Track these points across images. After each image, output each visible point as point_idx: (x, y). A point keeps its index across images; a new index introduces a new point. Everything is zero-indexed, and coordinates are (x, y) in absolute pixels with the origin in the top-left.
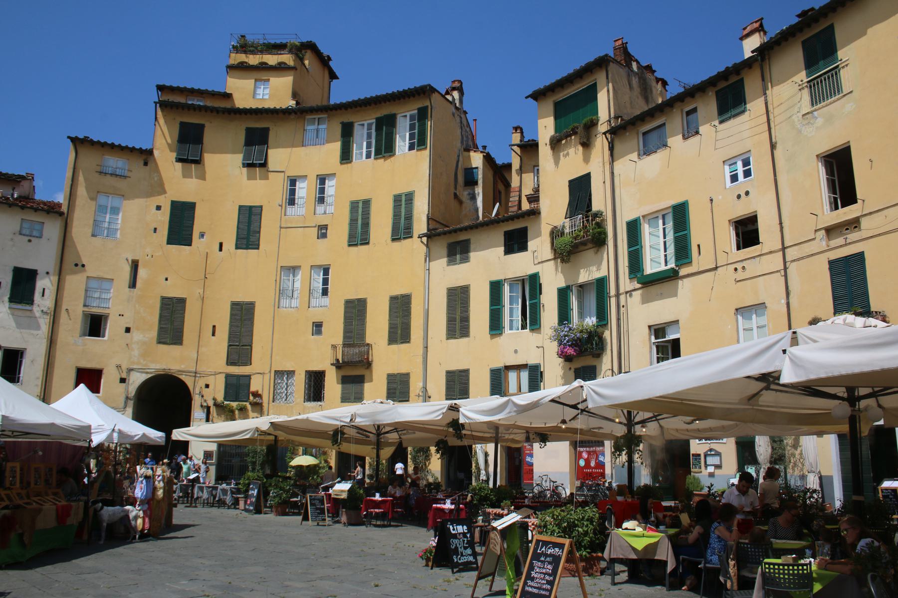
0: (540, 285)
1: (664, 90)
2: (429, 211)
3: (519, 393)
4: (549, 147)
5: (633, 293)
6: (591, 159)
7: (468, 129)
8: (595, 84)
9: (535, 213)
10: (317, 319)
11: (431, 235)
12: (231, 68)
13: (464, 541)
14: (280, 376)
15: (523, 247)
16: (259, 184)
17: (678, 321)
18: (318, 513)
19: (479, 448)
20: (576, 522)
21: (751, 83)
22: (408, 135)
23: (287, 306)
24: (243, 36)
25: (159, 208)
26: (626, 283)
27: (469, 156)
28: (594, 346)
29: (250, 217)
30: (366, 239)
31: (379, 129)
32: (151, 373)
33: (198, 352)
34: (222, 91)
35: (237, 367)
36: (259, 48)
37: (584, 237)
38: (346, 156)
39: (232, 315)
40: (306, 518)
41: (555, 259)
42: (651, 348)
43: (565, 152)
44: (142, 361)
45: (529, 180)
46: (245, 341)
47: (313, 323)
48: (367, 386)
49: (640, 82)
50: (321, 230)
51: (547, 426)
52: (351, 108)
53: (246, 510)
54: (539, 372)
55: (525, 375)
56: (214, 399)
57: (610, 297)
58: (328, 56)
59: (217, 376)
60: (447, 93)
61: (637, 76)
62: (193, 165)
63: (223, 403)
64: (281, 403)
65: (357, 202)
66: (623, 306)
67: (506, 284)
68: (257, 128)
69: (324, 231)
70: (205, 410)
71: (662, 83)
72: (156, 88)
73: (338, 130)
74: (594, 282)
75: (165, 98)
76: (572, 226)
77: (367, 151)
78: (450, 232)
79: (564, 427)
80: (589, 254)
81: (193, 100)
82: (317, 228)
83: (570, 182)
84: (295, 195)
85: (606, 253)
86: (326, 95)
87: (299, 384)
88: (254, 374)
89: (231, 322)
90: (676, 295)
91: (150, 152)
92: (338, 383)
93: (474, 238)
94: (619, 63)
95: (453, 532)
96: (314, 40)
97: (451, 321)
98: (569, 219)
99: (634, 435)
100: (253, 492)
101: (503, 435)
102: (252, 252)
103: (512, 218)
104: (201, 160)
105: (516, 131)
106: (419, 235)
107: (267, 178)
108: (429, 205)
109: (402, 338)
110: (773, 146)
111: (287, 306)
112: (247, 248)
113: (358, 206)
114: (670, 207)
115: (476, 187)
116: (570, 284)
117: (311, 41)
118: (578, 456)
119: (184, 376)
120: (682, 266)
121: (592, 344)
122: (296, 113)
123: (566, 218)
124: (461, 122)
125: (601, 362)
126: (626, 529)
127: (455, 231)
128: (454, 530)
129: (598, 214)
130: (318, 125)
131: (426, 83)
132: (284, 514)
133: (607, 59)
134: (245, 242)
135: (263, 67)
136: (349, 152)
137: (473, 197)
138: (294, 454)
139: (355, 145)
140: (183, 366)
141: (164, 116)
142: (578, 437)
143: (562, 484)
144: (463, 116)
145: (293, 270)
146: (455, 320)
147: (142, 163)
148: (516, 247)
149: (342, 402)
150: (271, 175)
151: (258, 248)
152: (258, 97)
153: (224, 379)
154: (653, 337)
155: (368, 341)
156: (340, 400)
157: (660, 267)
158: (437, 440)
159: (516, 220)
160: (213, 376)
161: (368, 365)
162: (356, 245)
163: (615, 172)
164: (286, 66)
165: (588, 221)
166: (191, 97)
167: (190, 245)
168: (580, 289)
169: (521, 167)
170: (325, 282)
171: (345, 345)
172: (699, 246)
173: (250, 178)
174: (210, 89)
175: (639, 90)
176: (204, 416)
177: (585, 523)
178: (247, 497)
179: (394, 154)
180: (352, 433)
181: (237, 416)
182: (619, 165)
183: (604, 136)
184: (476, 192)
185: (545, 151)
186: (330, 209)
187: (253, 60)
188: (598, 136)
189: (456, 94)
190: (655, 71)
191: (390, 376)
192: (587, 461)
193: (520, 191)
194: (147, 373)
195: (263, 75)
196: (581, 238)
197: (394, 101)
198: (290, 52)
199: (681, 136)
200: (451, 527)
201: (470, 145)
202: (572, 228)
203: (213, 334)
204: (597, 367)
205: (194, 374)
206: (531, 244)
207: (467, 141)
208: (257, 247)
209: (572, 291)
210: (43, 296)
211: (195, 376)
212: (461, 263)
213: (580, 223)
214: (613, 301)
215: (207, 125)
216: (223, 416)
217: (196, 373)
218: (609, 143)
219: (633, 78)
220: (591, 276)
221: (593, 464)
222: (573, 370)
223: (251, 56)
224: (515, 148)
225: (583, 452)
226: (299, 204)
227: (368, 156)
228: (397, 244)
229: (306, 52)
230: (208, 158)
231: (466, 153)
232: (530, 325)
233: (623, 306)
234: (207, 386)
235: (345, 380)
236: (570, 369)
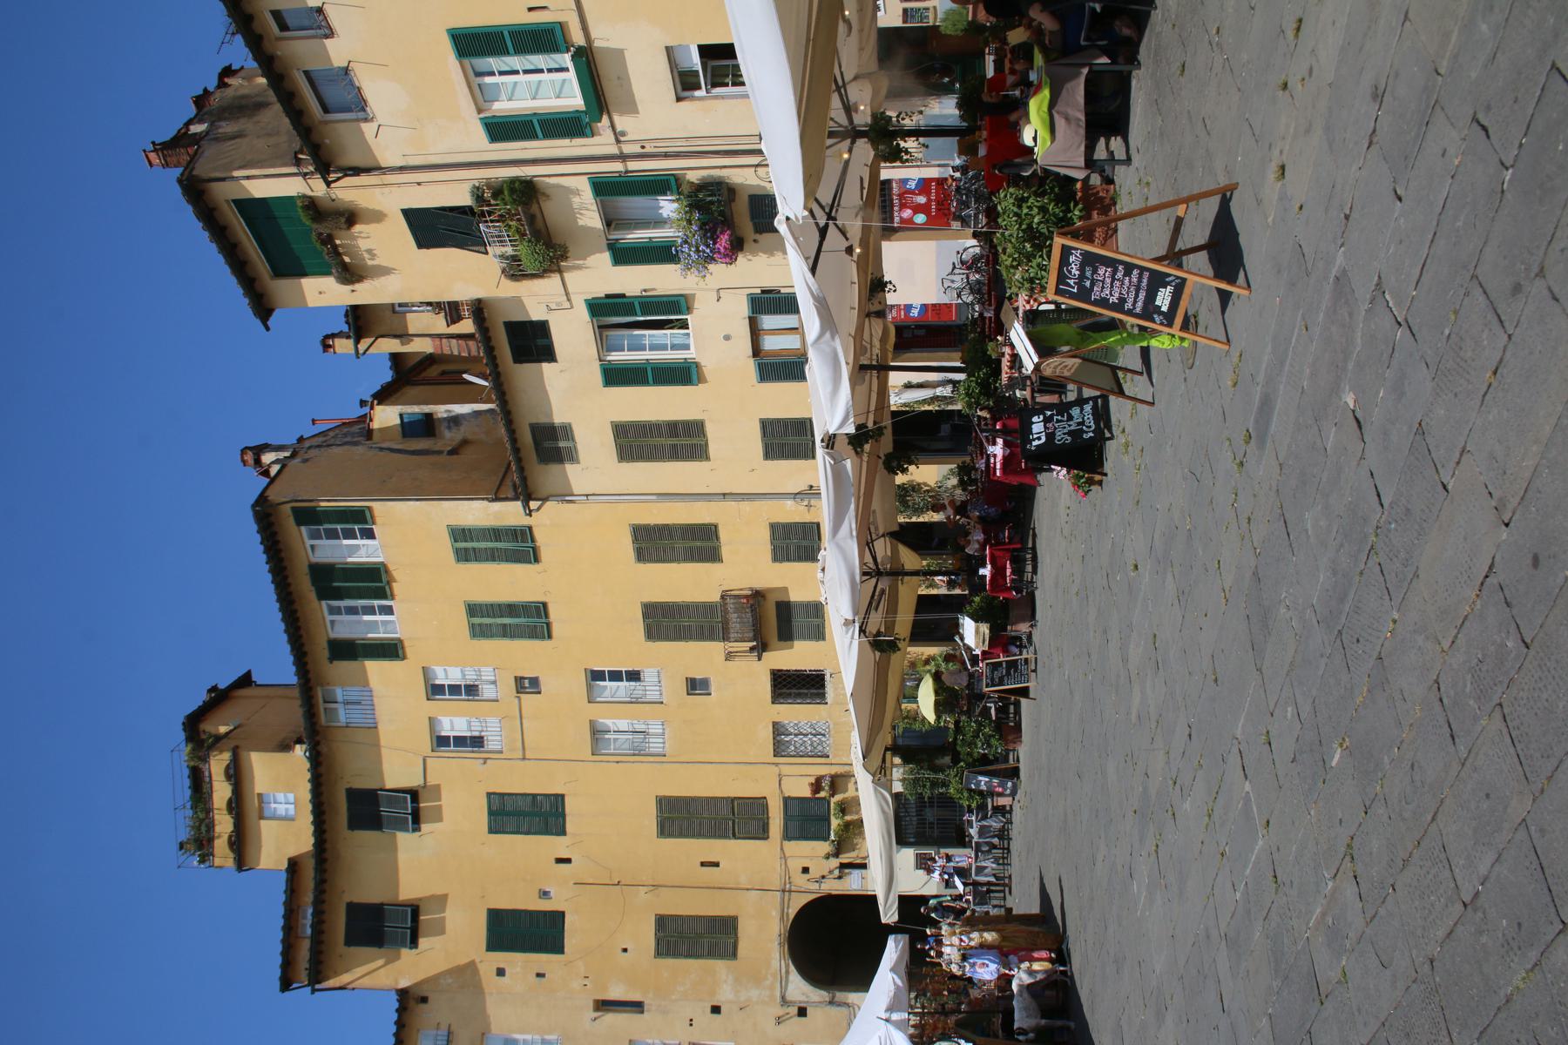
0: (608, 296)
1: (242, 74)
2: (483, 499)
3: (800, 330)
4: (357, 286)
5: (619, 128)
6: (377, 208)
7: (332, 434)
8: (236, 202)
9: (479, 309)
10: (682, 687)
11: (526, 493)
12: (241, 864)
13: (1058, 421)
14: (783, 747)
15: (542, 328)
16: (447, 801)
17: (667, 48)
18: (1015, 671)
19: (897, 399)
20: (1024, 227)
22: (346, 542)
23: (661, 740)
24: (181, 846)
25: (501, 972)
26: (601, 142)
27: (381, 430)
28: (715, 199)
29: (509, 814)
30: (537, 608)
31: (339, 594)
32: (787, 966)
33: (748, 889)
34: (284, 876)
35: (771, 821)
36: (202, 816)
37: (519, 220)
38: (390, 650)
39: (681, 835)
40: (1024, 692)
41: (560, 271)
42: (716, 97)
43: (366, 256)
44: (768, 982)
45: (420, 321)
47: (688, 694)
48: (795, 596)
49: (225, 119)
50: (526, 688)
51: (856, 280)
52: (302, 645)
53: (1013, 794)
54: (763, 296)
55: (769, 321)
56: (827, 857)
57: (627, 172)
58: (210, 691)
59: (787, 855)
60: (266, 473)
61: (216, 123)
62: (422, 918)
63: (833, 841)
64: (830, 745)
65: (472, 627)
66: (643, 147)
67: (609, 358)
68: (349, 809)
69: (527, 683)
70: (847, 871)
71: (228, 76)
72: (287, 993)
73: (344, 667)
74: (601, 200)
75: (304, 976)
76: (502, 241)
77: (380, 614)
78: (519, 460)
79: (858, 250)
80: (551, 210)
81: (305, 925)
82: (522, 696)
83: (420, 245)
84: (465, 737)
85: (547, 180)
86: (280, 691)
87: (796, 714)
88: (782, 792)
89: (693, 836)
90: (620, 53)
91: (403, 994)
92: (792, 647)
93: (527, 417)
94: (193, 158)
95: (1043, 439)
96: (182, 719)
97: (675, 454)
98: (488, 248)
99: (871, 126)
100: (983, 783)
101: (875, 357)
102: (570, 806)
103: (490, 350)
104: (412, 905)
105: (330, 346)
106: (527, 515)
107: (437, 788)
108: (472, 499)
109: (710, 539)
111: (661, 740)
112: (563, 815)
113: (480, 625)
114: (461, 63)
115: (435, 417)
116: (605, 242)
117: (184, 724)
118: (908, 227)
119: (790, 911)
120: (568, 38)
121: (712, 203)
122: (318, 743)
123: (487, 253)
124: (319, 446)
125: (742, 184)
126: (1035, 139)
127: (516, 451)
128: (1039, 438)
129: (478, 194)
130: (336, 702)
131: (250, 515)
132: (1018, 728)
133: (187, 179)
134: (552, 820)
135: (237, 806)
136: (382, 645)
137: (455, 421)
138: (915, 716)
139: (370, 635)
140: (774, 913)
141: (336, 974)
142: (876, 224)
143: (958, 253)
144: (307, 444)
145: (597, 733)
146: (674, 446)
147: (423, 1006)
148: (540, 342)
149: (824, 639)
150: (431, 781)
152: (292, 812)
153: (793, 843)
154: (697, 93)
155: (716, 598)
156: (821, 643)
157: (571, 80)
158: (885, 471)
159: (493, 343)
160: (788, 862)
161: (758, 596)
162: (548, 625)
164: (232, 766)
165: (490, 213)
166: (299, 930)
167: (563, 913)
168: (613, 226)
169: (395, 336)
170: (616, 676)
171: (725, 638)
172: (530, 9)
173: (438, 816)
174: (283, 898)
175: (243, 121)
176: (856, 873)
177: (1025, 211)
178: (992, 794)
179: (383, 564)
180: (876, 621)
181: (855, 817)
182: (387, 158)
183: (333, 185)
184: (445, 415)
185: (366, 293)
186: (487, 673)
187: (224, 824)
188: (334, 197)
189: (268, 458)
190: (205, 90)
192: (918, 209)
193: (440, 336)
194: (787, 972)
195: (252, 805)
196: (522, 225)
197: (285, 568)
198: (205, 759)
199: (328, 42)
200: (1035, 443)
201: (361, 429)
202: (503, 236)
203: (716, 865)
204: (752, 192)
205: (787, 894)
206: (536, 315)
207: (353, 435)
208: (559, 799)
209: (617, 240)
211: (790, 891)
212: (573, 440)
213: (494, 227)
214: (633, 165)
215: (348, 898)
216: (855, 841)
217: (784, 891)
218: (346, 175)
219: (220, 130)
220: (589, 206)
221: (922, 200)
222: (758, 237)
223: (218, 829)
224: (362, 346)
225: (901, 218)
226: (480, 729)
227: (388, 610)
228: (544, 554)
229: (204, 731)
230: (407, 892)
231: (376, 436)
232: (680, 313)
233: (643, 147)
234: (806, 870)
235: (786, 634)
236: (755, 241)
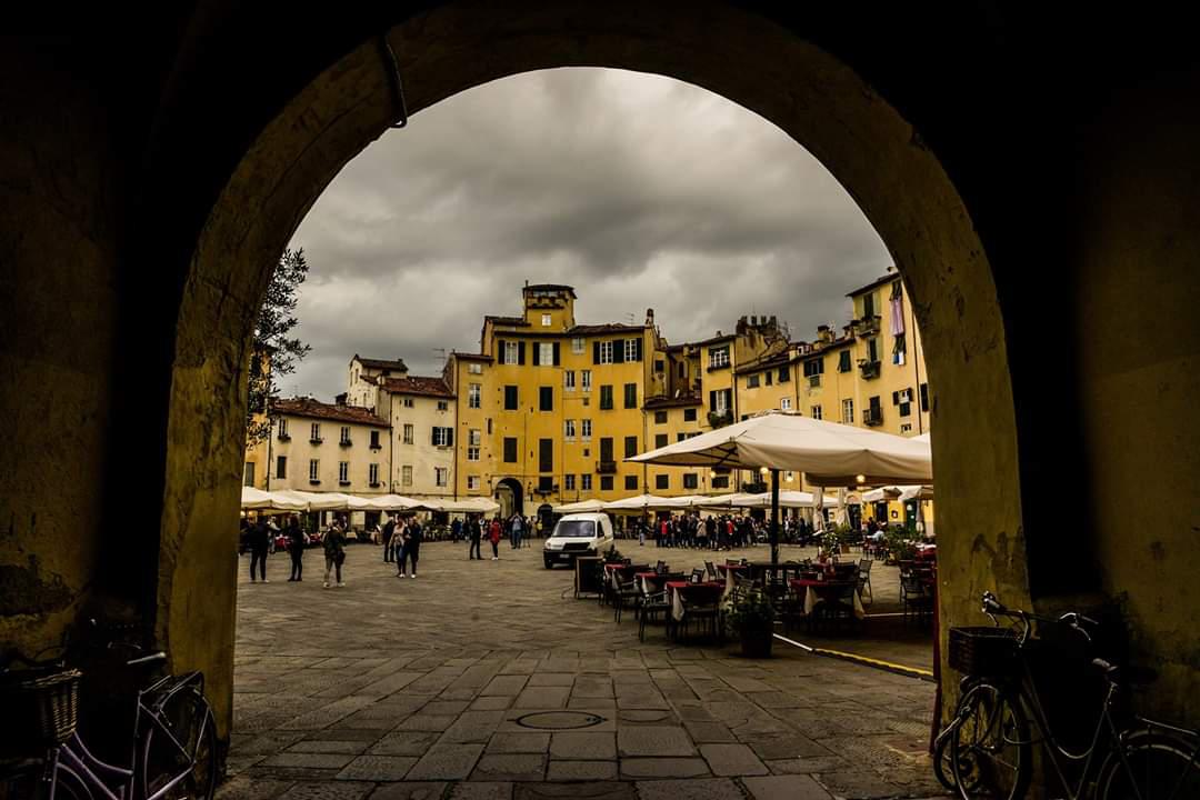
11: (647, 408)
21: (792, 372)
38: (596, 361)
110: (798, 398)
191: (627, 477)
227: (609, 361)
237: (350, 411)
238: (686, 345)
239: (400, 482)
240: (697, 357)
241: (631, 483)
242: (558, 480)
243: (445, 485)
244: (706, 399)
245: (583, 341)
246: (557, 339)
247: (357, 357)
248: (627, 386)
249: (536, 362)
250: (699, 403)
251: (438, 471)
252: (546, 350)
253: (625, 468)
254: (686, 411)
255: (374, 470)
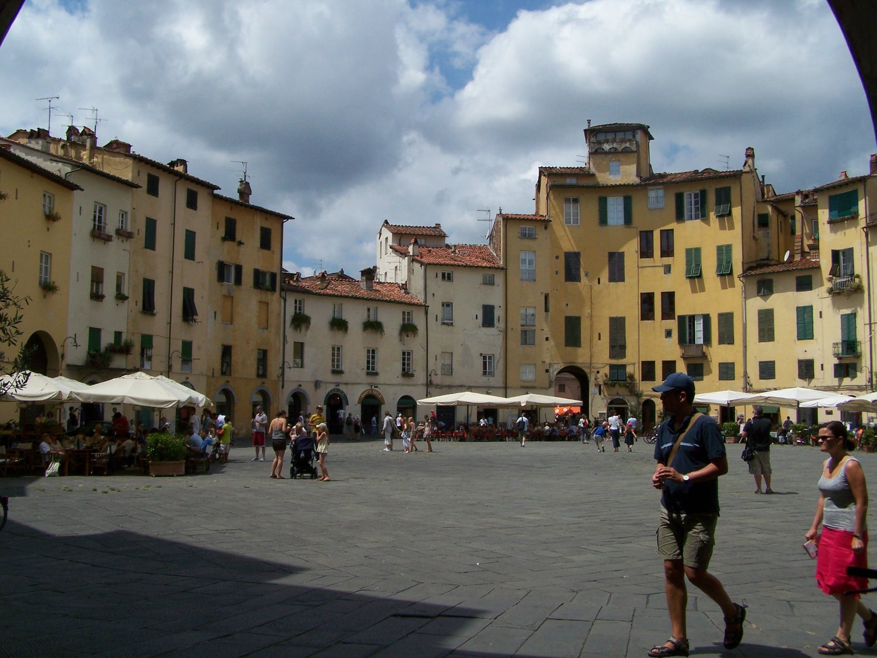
10: (668, 328)
46: (620, 343)
93: (774, 278)
113: (692, 253)
151: (624, 281)
163: (869, 252)
176: (597, 390)
203: (600, 339)
210: (499, 321)
237: (378, 287)
238: (798, 193)
239: (439, 372)
240: (810, 209)
241: (727, 372)
242: (634, 370)
243: (492, 374)
244: (826, 263)
245: (661, 193)
246: (626, 192)
247: (386, 222)
248: (720, 249)
249: (603, 220)
250: (817, 268)
251: (485, 358)
252: (615, 208)
253: (718, 353)
254: (798, 278)
255: (406, 357)
